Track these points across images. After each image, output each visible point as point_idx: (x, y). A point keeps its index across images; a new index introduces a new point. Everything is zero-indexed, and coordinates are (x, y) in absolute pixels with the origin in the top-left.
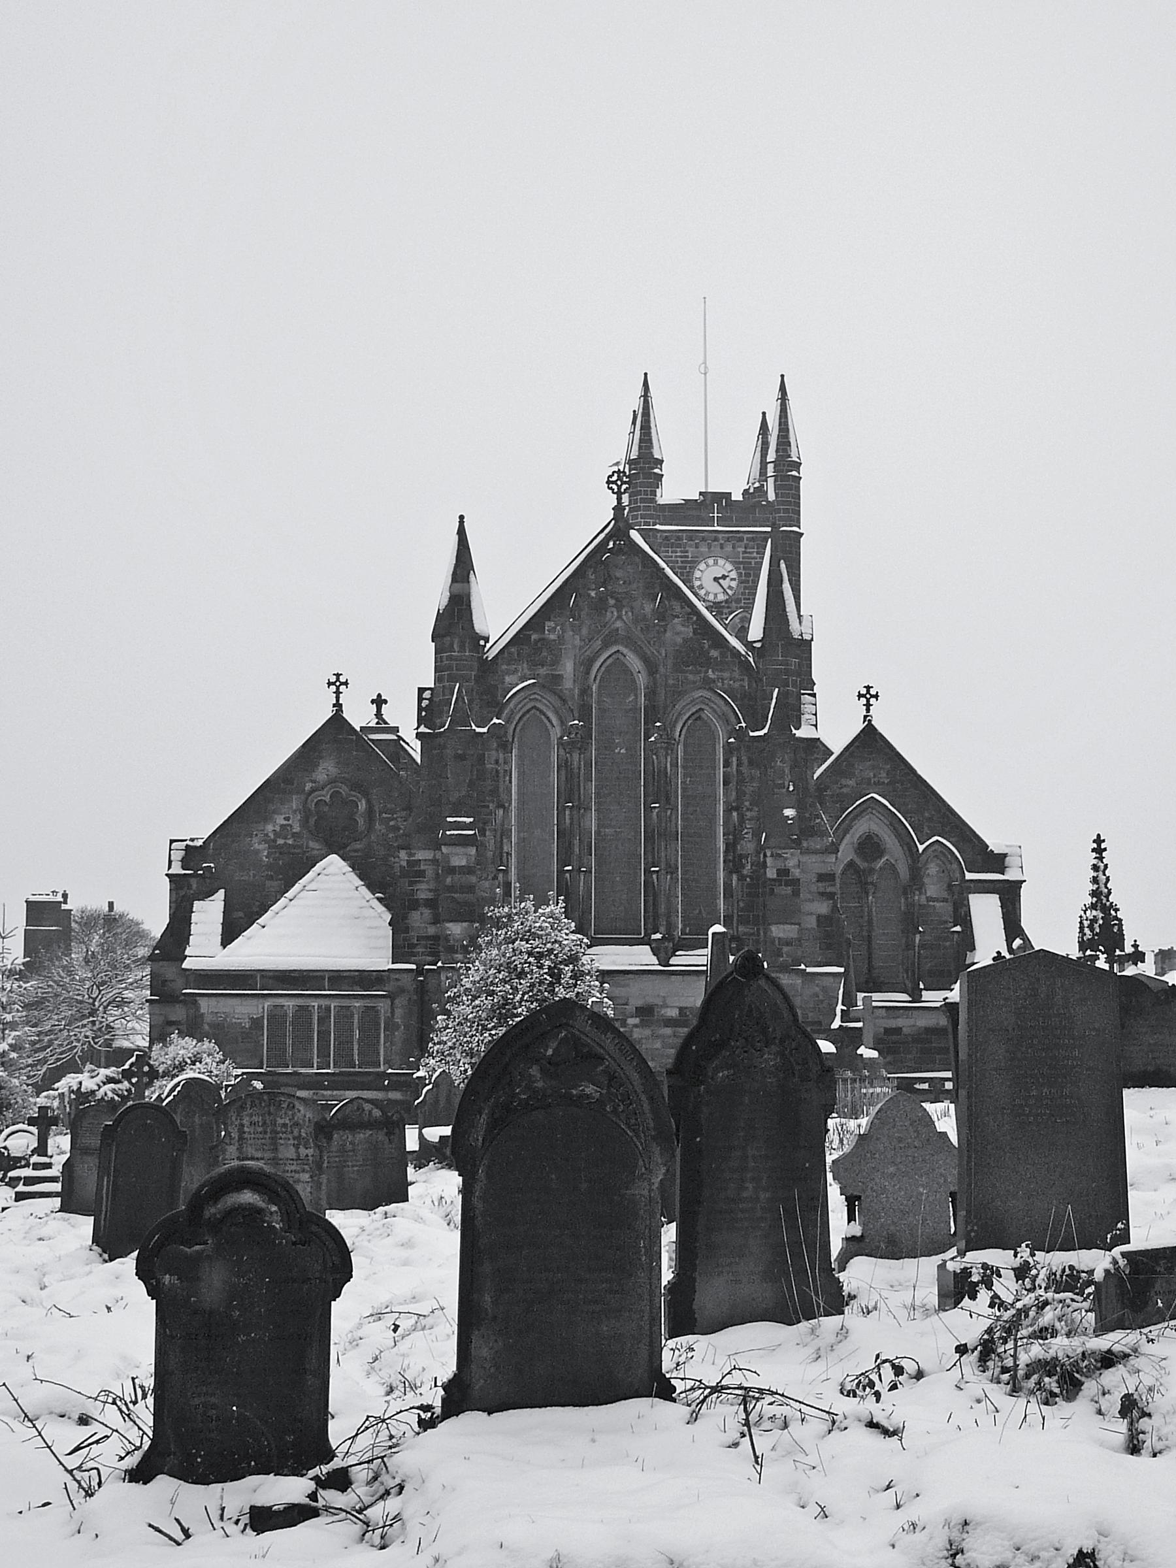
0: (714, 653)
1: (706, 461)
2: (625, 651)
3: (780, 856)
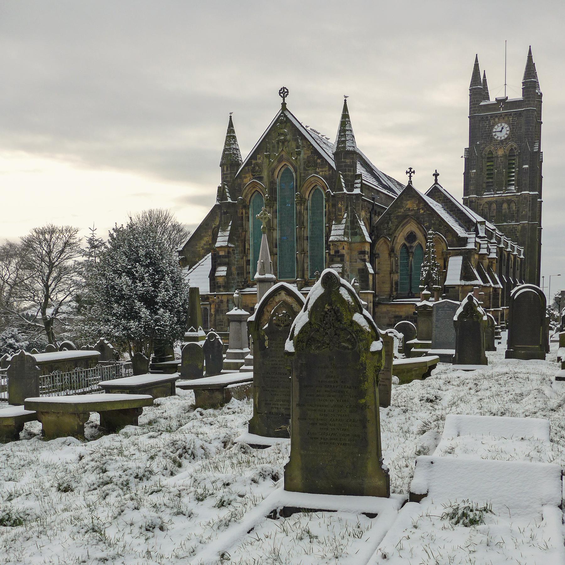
0: (319, 161)
1: (505, 86)
2: (288, 164)
3: (335, 245)
